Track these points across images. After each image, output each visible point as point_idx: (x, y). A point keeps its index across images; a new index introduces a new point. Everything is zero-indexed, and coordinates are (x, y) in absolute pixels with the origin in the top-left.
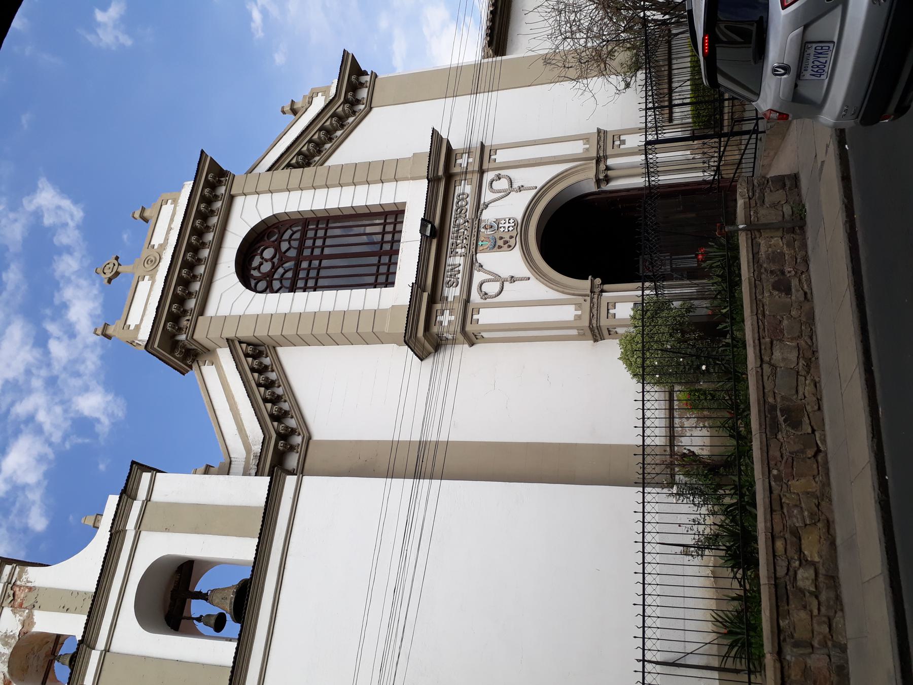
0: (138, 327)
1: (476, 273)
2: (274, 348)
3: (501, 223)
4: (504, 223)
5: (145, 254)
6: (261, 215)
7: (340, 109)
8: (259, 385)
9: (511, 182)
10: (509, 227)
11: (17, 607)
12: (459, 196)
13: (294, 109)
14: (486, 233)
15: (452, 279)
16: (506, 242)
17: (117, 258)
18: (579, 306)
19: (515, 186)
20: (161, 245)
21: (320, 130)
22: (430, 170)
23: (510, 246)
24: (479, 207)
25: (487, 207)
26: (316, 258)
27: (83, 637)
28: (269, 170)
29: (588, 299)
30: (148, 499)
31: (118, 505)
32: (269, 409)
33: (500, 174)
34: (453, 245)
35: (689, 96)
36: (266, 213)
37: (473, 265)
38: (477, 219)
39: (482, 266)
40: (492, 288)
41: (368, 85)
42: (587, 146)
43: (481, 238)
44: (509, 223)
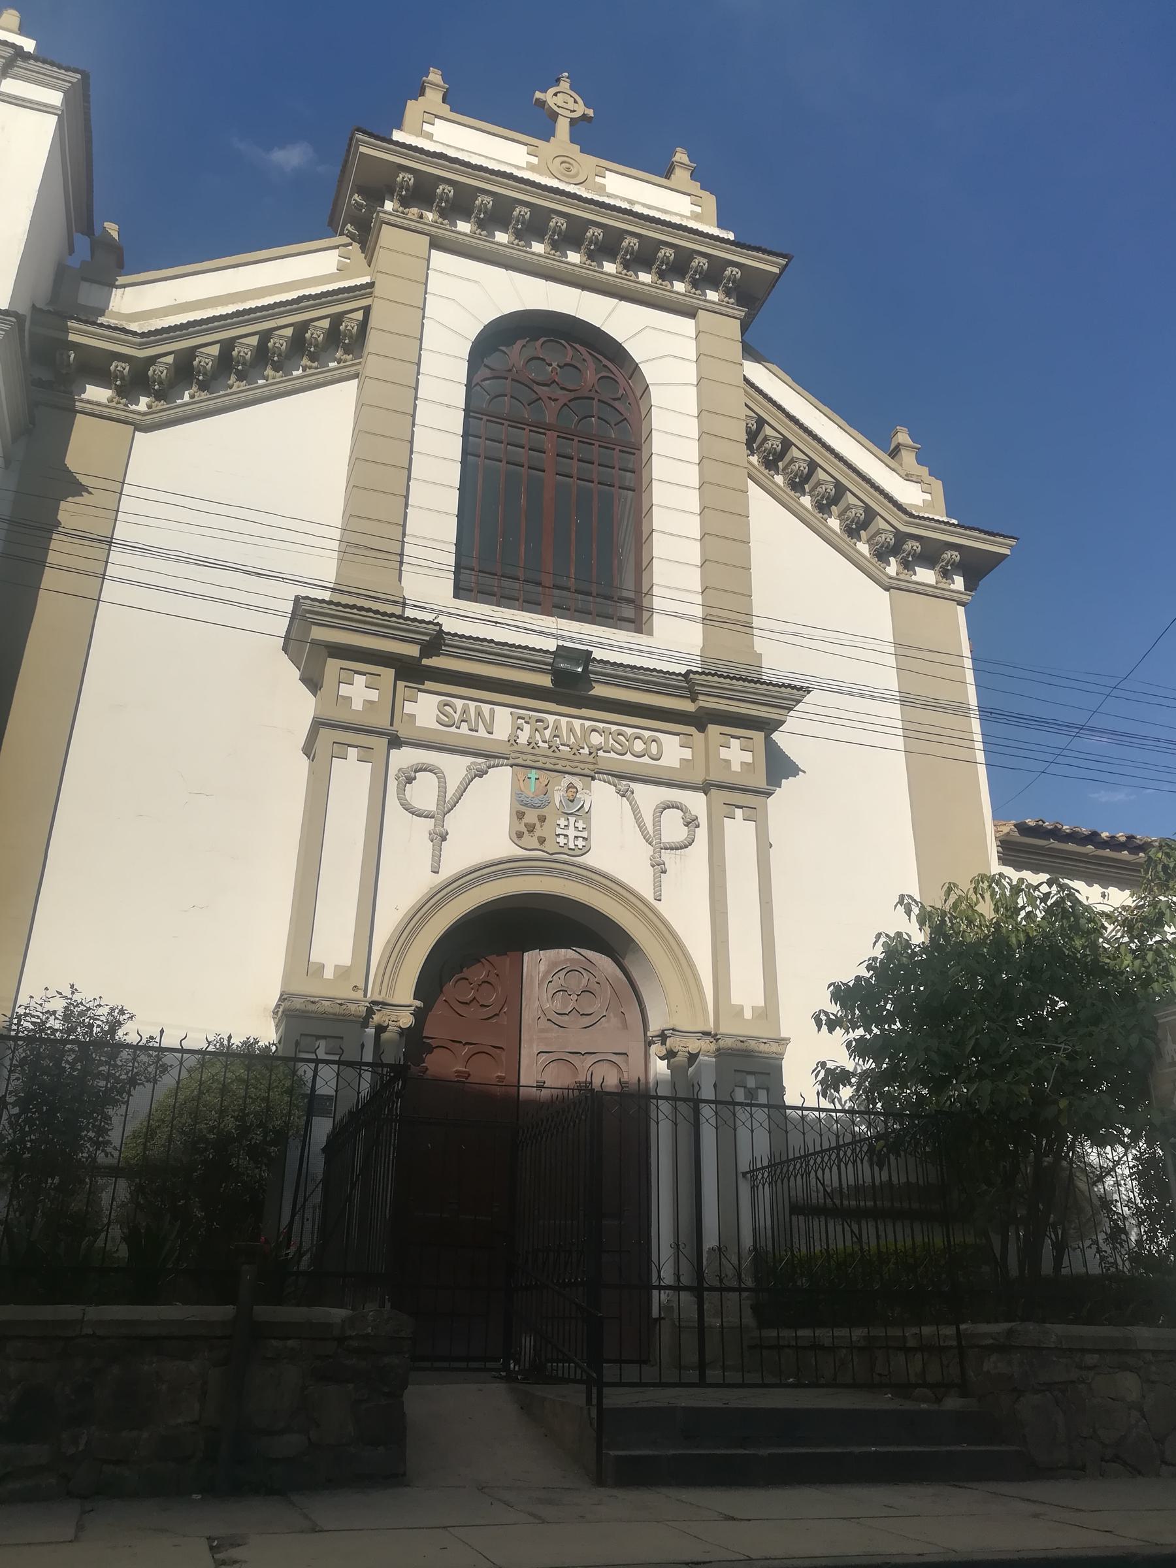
1: (468, 760)
2: (356, 376)
5: (590, 161)
6: (628, 342)
7: (882, 525)
8: (266, 336)
9: (677, 849)
10: (566, 836)
12: (653, 741)
13: (900, 450)
14: (556, 788)
15: (456, 716)
16: (531, 828)
17: (584, 117)
18: (343, 973)
19: (667, 856)
20: (603, 187)
21: (838, 485)
22: (710, 678)
23: (520, 835)
24: (622, 777)
25: (623, 796)
28: (746, 379)
29: (359, 995)
33: (698, 826)
34: (537, 721)
35: (832, 1246)
36: (649, 372)
38: (592, 773)
39: (481, 776)
40: (424, 793)
41: (940, 585)
42: (748, 1015)
43: (544, 777)
44: (576, 837)
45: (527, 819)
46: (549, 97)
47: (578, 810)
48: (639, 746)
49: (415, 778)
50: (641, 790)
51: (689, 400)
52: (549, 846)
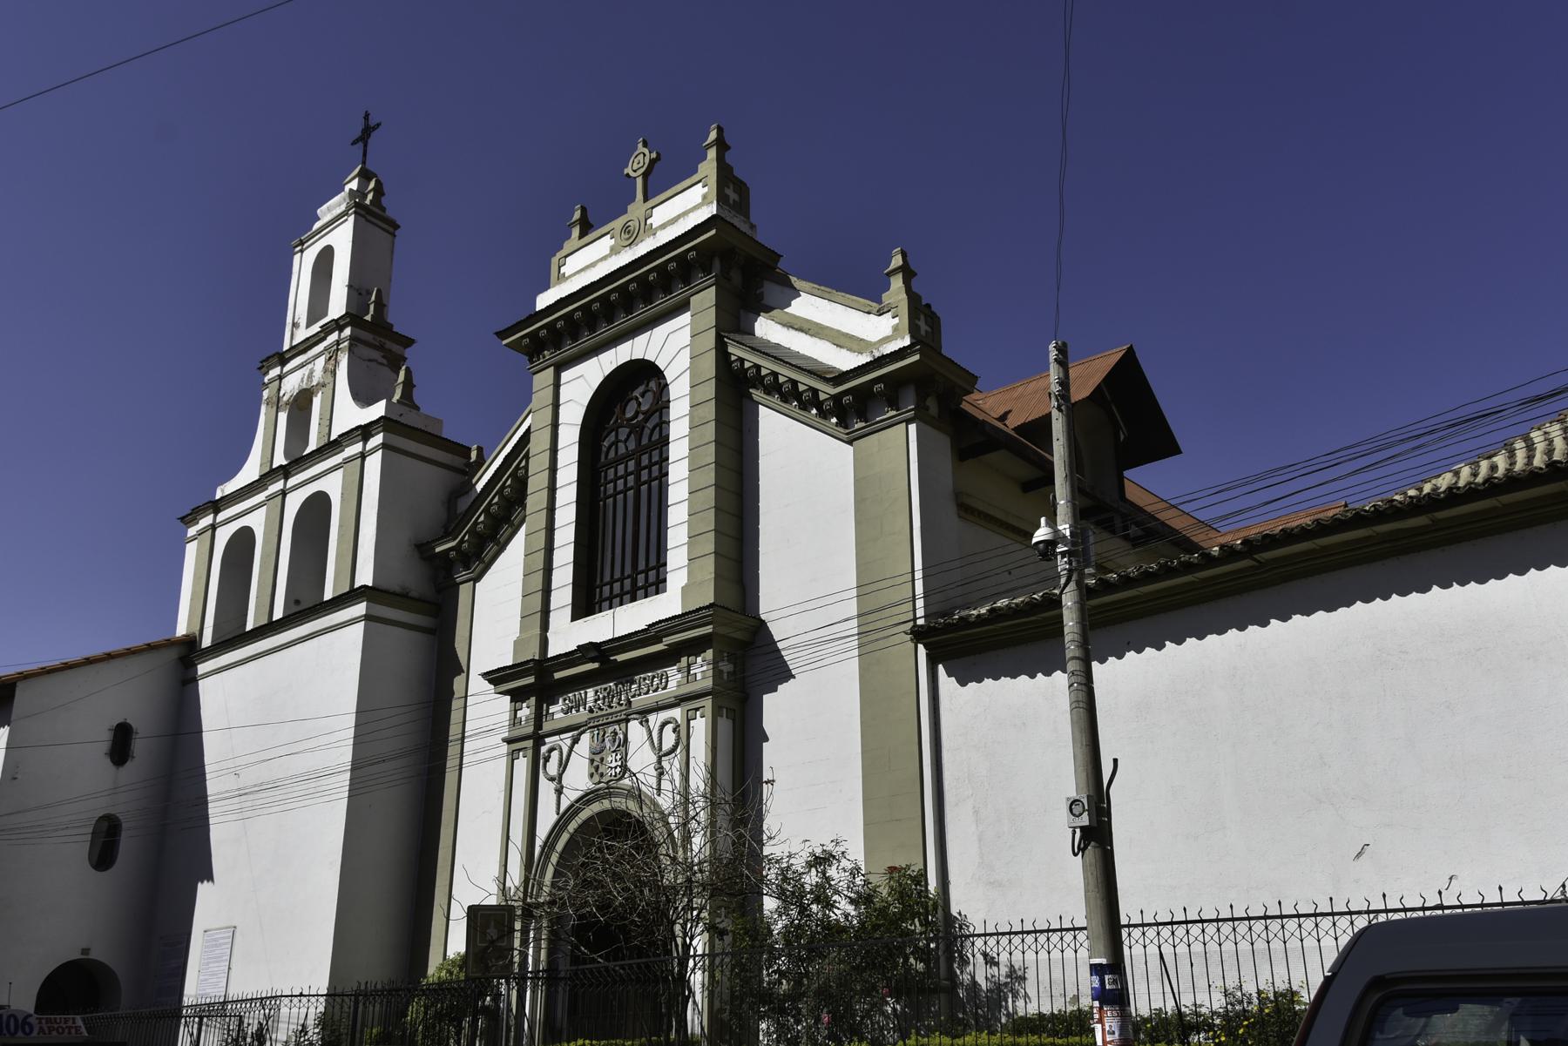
0: (562, 278)
1: (570, 734)
3: (616, 755)
4: (616, 761)
8: (500, 492)
11: (325, 370)
16: (597, 768)
17: (652, 162)
21: (791, 380)
23: (591, 776)
24: (644, 713)
26: (638, 478)
27: (286, 465)
30: (363, 456)
31: (352, 430)
32: (479, 521)
36: (669, 375)
37: (576, 729)
45: (595, 763)
46: (628, 170)
47: (619, 746)
48: (656, 681)
49: (549, 757)
50: (652, 718)
51: (685, 382)
52: (604, 780)
